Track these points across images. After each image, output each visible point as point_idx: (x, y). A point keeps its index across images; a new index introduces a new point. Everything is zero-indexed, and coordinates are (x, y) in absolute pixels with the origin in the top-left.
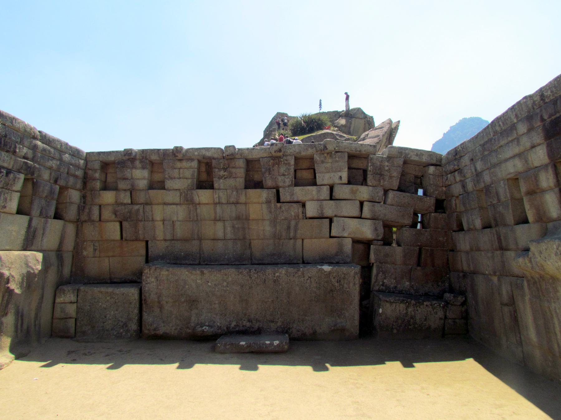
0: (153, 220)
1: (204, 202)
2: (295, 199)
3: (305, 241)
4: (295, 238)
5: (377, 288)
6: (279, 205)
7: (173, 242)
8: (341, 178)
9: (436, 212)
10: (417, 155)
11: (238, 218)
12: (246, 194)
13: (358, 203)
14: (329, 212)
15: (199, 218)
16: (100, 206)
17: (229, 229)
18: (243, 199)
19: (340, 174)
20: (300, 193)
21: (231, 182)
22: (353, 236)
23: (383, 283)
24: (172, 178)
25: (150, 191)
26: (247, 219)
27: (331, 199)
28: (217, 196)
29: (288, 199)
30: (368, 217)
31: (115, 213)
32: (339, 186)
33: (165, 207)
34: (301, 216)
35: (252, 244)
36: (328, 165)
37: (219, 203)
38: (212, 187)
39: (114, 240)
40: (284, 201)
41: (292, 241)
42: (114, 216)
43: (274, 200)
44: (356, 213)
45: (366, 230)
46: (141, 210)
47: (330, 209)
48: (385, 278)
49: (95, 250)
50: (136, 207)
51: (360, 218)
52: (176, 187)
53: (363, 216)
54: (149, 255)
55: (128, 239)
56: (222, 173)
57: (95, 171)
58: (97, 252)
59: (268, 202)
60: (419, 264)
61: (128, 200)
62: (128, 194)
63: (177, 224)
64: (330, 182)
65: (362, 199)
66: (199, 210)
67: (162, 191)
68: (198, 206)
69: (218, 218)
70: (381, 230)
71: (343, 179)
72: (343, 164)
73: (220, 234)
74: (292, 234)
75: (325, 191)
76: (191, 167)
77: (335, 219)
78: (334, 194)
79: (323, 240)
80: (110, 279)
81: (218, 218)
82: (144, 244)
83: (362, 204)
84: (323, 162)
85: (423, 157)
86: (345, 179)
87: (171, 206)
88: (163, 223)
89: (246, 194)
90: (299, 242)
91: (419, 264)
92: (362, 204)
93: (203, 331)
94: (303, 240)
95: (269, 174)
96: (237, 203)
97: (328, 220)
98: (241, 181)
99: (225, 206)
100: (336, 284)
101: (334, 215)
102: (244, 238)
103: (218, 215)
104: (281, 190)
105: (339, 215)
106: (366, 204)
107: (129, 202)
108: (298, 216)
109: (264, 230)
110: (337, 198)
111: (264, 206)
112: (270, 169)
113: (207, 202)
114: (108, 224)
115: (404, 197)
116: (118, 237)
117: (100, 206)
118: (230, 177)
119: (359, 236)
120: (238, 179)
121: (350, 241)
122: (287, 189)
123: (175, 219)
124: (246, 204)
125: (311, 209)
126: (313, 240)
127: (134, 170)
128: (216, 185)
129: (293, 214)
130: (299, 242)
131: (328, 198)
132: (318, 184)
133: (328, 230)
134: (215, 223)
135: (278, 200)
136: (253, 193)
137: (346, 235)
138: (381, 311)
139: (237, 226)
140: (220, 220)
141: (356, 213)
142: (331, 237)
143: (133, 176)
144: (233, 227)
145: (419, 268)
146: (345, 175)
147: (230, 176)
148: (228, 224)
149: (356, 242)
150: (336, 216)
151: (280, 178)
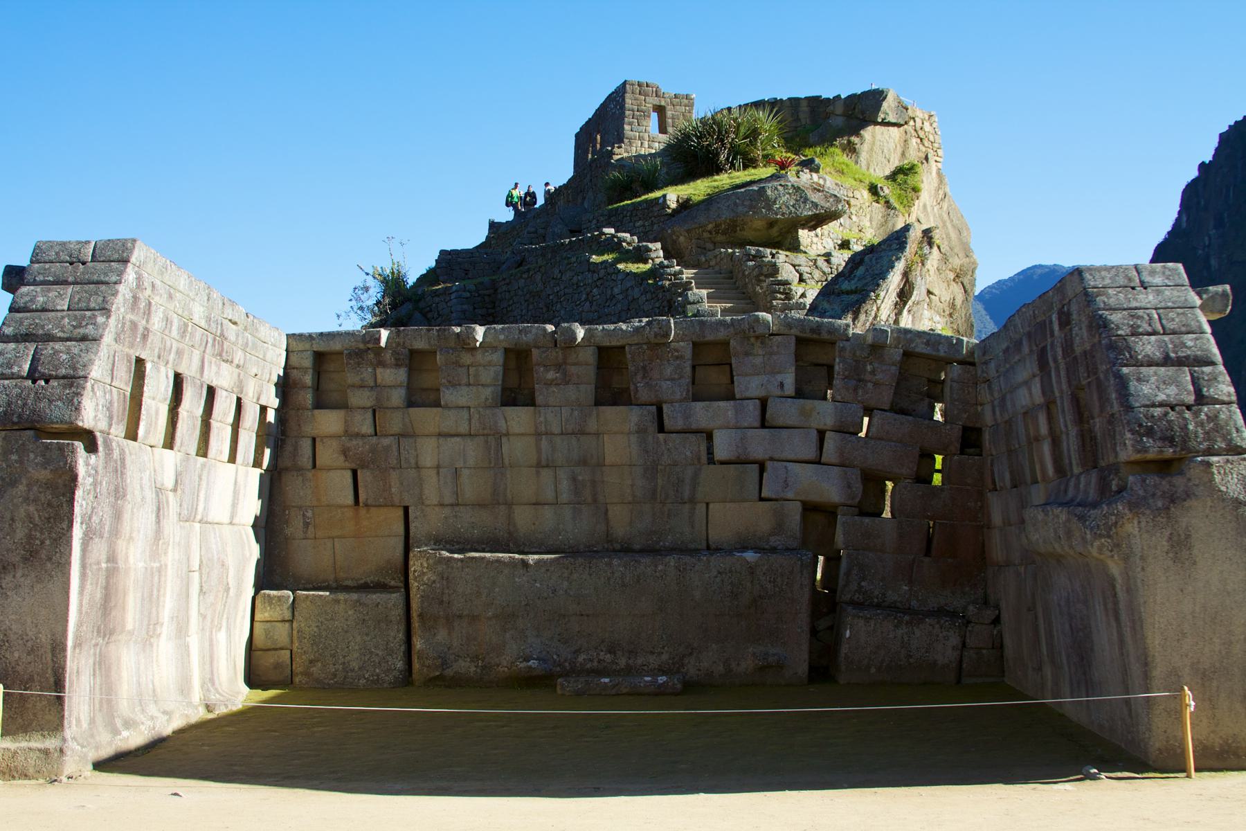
0: (417, 467)
1: (517, 431)
2: (694, 426)
3: (711, 506)
4: (692, 501)
5: (847, 597)
6: (661, 436)
7: (457, 509)
8: (782, 385)
9: (962, 453)
10: (927, 344)
11: (583, 462)
12: (598, 415)
13: (814, 434)
14: (758, 452)
15: (506, 462)
16: (314, 440)
17: (565, 485)
18: (592, 426)
19: (779, 378)
20: (702, 414)
21: (571, 392)
22: (803, 498)
23: (860, 587)
24: (454, 386)
25: (411, 410)
26: (601, 464)
27: (763, 425)
28: (542, 419)
29: (680, 425)
30: (833, 461)
31: (345, 452)
32: (778, 400)
33: (441, 440)
34: (704, 458)
35: (610, 513)
36: (758, 361)
37: (546, 434)
38: (531, 402)
39: (341, 507)
40: (672, 429)
41: (687, 506)
42: (342, 458)
43: (653, 428)
44: (811, 453)
45: (829, 487)
46: (395, 448)
47: (759, 444)
48: (864, 579)
49: (307, 525)
50: (386, 441)
51: (819, 463)
52: (463, 401)
53: (823, 460)
54: (412, 534)
55: (369, 502)
56: (551, 375)
57: (305, 370)
58: (311, 528)
59: (641, 431)
60: (928, 553)
61: (367, 428)
62: (369, 415)
63: (465, 472)
64: (762, 393)
65: (821, 427)
66: (505, 449)
67: (435, 410)
68: (504, 440)
69: (544, 463)
70: (858, 487)
71: (786, 387)
72: (786, 357)
73: (549, 495)
74: (687, 494)
75: (752, 408)
76: (490, 364)
77: (769, 465)
78: (768, 416)
79: (746, 504)
80: (336, 580)
81: (544, 463)
82: (401, 512)
83: (821, 434)
84: (747, 354)
85: (940, 347)
86: (790, 388)
87: (453, 440)
88: (438, 473)
89: (598, 415)
90: (701, 508)
91: (928, 553)
92: (821, 434)
93: (530, 667)
94: (708, 504)
95: (644, 377)
96: (583, 433)
97: (756, 466)
98: (587, 391)
99: (558, 440)
100: (769, 586)
101: (767, 457)
102: (595, 501)
103: (544, 456)
104: (665, 407)
105: (776, 456)
106: (828, 434)
107: (371, 431)
108: (699, 459)
109: (632, 486)
110: (774, 424)
111: (634, 438)
112: (644, 368)
113: (522, 430)
114: (331, 474)
115: (902, 424)
116: (350, 500)
117: (314, 440)
118: (567, 383)
119: (814, 497)
120: (582, 387)
121: (798, 506)
122: (677, 405)
123: (460, 464)
124: (597, 434)
125: (723, 446)
126: (728, 505)
127: (379, 370)
128: (539, 399)
129: (688, 453)
130: (701, 508)
131: (757, 424)
132: (738, 396)
133: (757, 487)
134: (538, 473)
135: (661, 429)
136: (611, 413)
137: (790, 495)
138: (848, 634)
139: (580, 478)
140: (547, 466)
141: (811, 453)
142: (761, 499)
143: (379, 381)
144: (574, 479)
145: (927, 560)
146: (789, 380)
147: (566, 380)
148: (563, 475)
149: (810, 508)
150: (772, 459)
151: (665, 385)
